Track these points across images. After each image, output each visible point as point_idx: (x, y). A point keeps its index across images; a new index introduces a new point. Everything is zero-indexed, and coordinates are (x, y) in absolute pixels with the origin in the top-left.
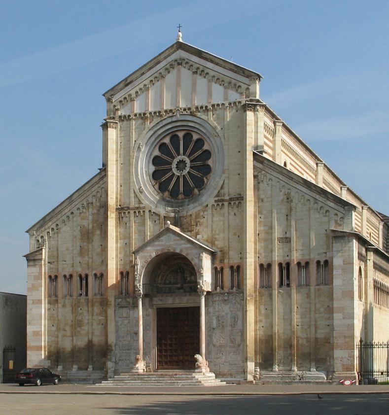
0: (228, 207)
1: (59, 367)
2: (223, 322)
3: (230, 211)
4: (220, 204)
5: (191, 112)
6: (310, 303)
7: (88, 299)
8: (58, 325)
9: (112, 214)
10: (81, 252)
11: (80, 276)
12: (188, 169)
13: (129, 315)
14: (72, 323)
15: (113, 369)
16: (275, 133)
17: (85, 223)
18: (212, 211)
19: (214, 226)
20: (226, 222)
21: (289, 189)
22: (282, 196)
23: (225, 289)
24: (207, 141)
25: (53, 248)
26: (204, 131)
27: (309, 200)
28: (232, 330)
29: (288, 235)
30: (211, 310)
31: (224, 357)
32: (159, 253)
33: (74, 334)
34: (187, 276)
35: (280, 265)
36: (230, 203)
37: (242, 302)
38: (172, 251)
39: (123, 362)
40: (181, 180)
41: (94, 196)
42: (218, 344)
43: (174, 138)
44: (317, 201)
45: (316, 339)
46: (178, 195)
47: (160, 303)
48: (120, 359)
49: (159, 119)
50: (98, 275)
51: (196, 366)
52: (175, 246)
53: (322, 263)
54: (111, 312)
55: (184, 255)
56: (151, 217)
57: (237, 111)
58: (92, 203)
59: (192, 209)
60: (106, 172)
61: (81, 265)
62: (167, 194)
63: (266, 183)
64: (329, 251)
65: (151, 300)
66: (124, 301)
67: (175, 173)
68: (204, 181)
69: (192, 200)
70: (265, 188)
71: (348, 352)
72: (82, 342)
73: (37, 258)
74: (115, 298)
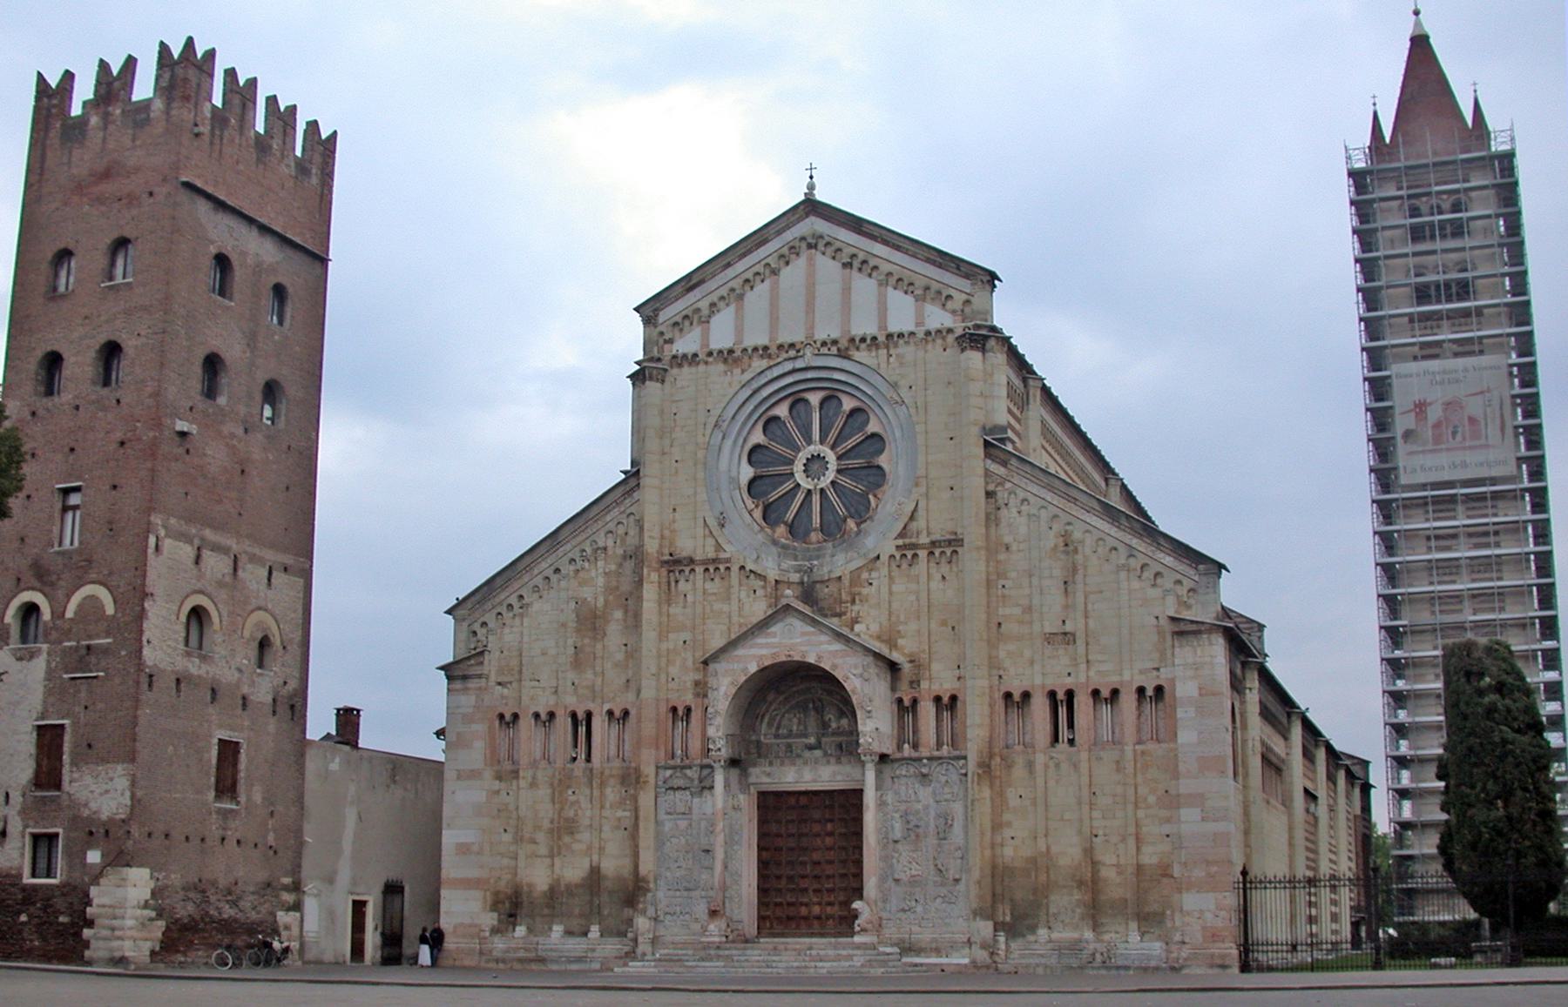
0: (928, 561)
1: (518, 928)
2: (917, 826)
3: (933, 570)
4: (909, 554)
5: (839, 350)
6: (1125, 784)
7: (591, 770)
8: (518, 829)
9: (652, 574)
10: (576, 660)
11: (574, 715)
12: (831, 475)
13: (690, 808)
14: (549, 826)
15: (651, 936)
16: (1028, 404)
17: (587, 593)
18: (890, 572)
19: (895, 605)
20: (924, 595)
21: (1069, 524)
22: (1051, 540)
23: (921, 749)
24: (876, 414)
25: (509, 650)
26: (869, 393)
27: (1115, 549)
28: (939, 845)
29: (1068, 627)
30: (889, 798)
31: (919, 909)
32: (766, 664)
33: (555, 850)
34: (830, 719)
35: (1052, 695)
36: (931, 553)
37: (964, 778)
38: (796, 658)
39: (675, 917)
40: (816, 498)
41: (611, 532)
42: (902, 876)
43: (798, 402)
44: (1136, 553)
45: (1139, 868)
46: (807, 533)
47: (768, 780)
48: (667, 910)
49: (765, 363)
50: (617, 713)
51: (857, 929)
52: (803, 648)
53: (1150, 692)
54: (646, 799)
55: (827, 668)
56: (745, 581)
57: (945, 350)
58: (605, 549)
59: (838, 563)
60: (638, 479)
61: (575, 690)
62: (781, 530)
63: (1014, 510)
64: (1166, 666)
65: (744, 774)
66: (678, 774)
67: (800, 482)
68: (869, 502)
69: (844, 541)
70: (1012, 520)
71: (1216, 899)
72: (573, 871)
73: (472, 671)
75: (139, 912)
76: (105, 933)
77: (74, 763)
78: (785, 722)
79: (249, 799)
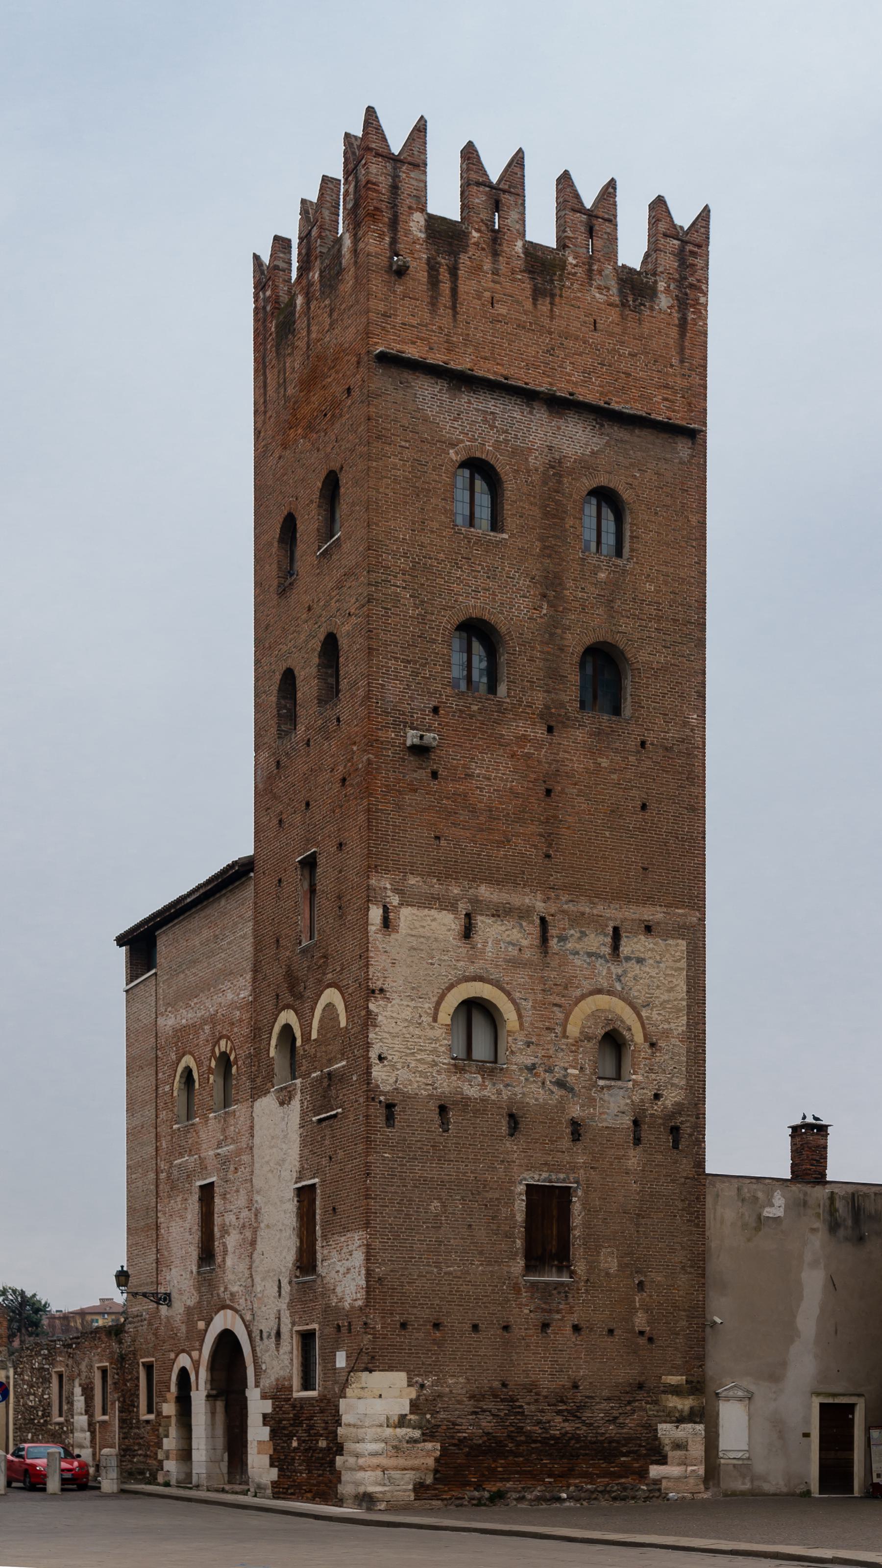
75: (389, 1431)
76: (352, 1460)
77: (324, 1237)
79: (592, 1267)
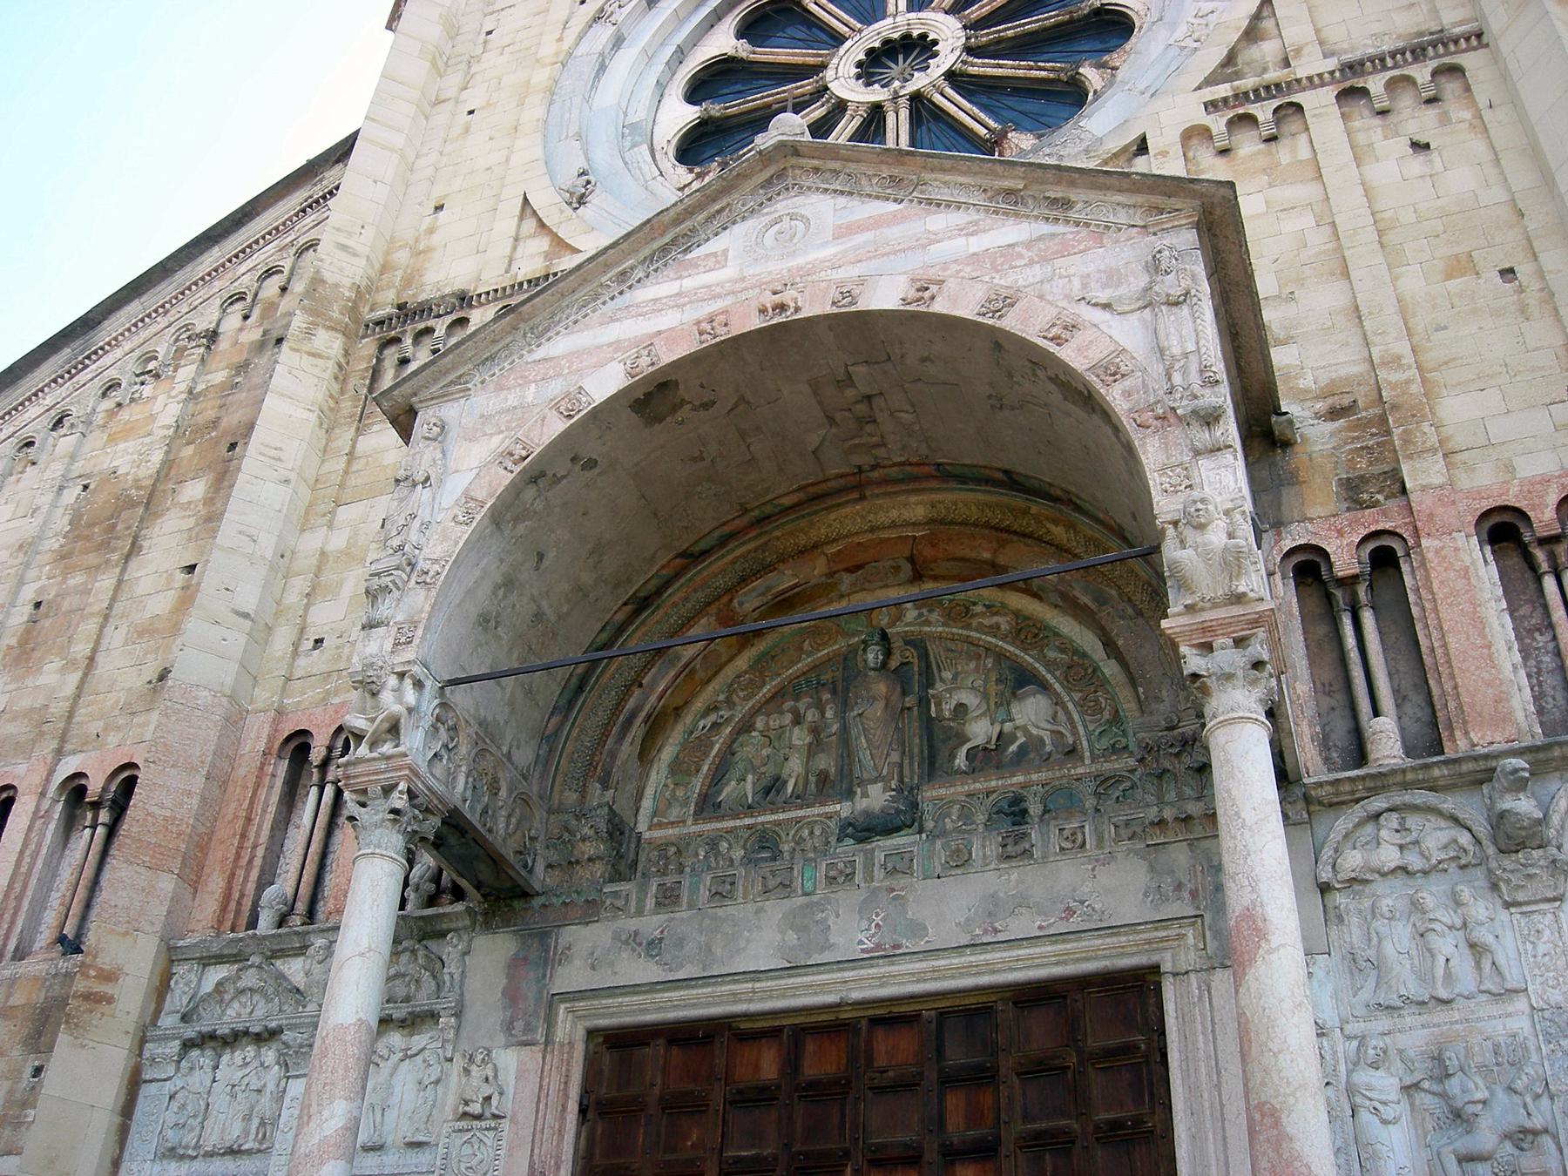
2: (1523, 1137)
13: (268, 1125)
32: (667, 357)
34: (961, 708)
38: (814, 306)
47: (647, 971)
66: (250, 979)
74: (171, 956)
78: (753, 748)
